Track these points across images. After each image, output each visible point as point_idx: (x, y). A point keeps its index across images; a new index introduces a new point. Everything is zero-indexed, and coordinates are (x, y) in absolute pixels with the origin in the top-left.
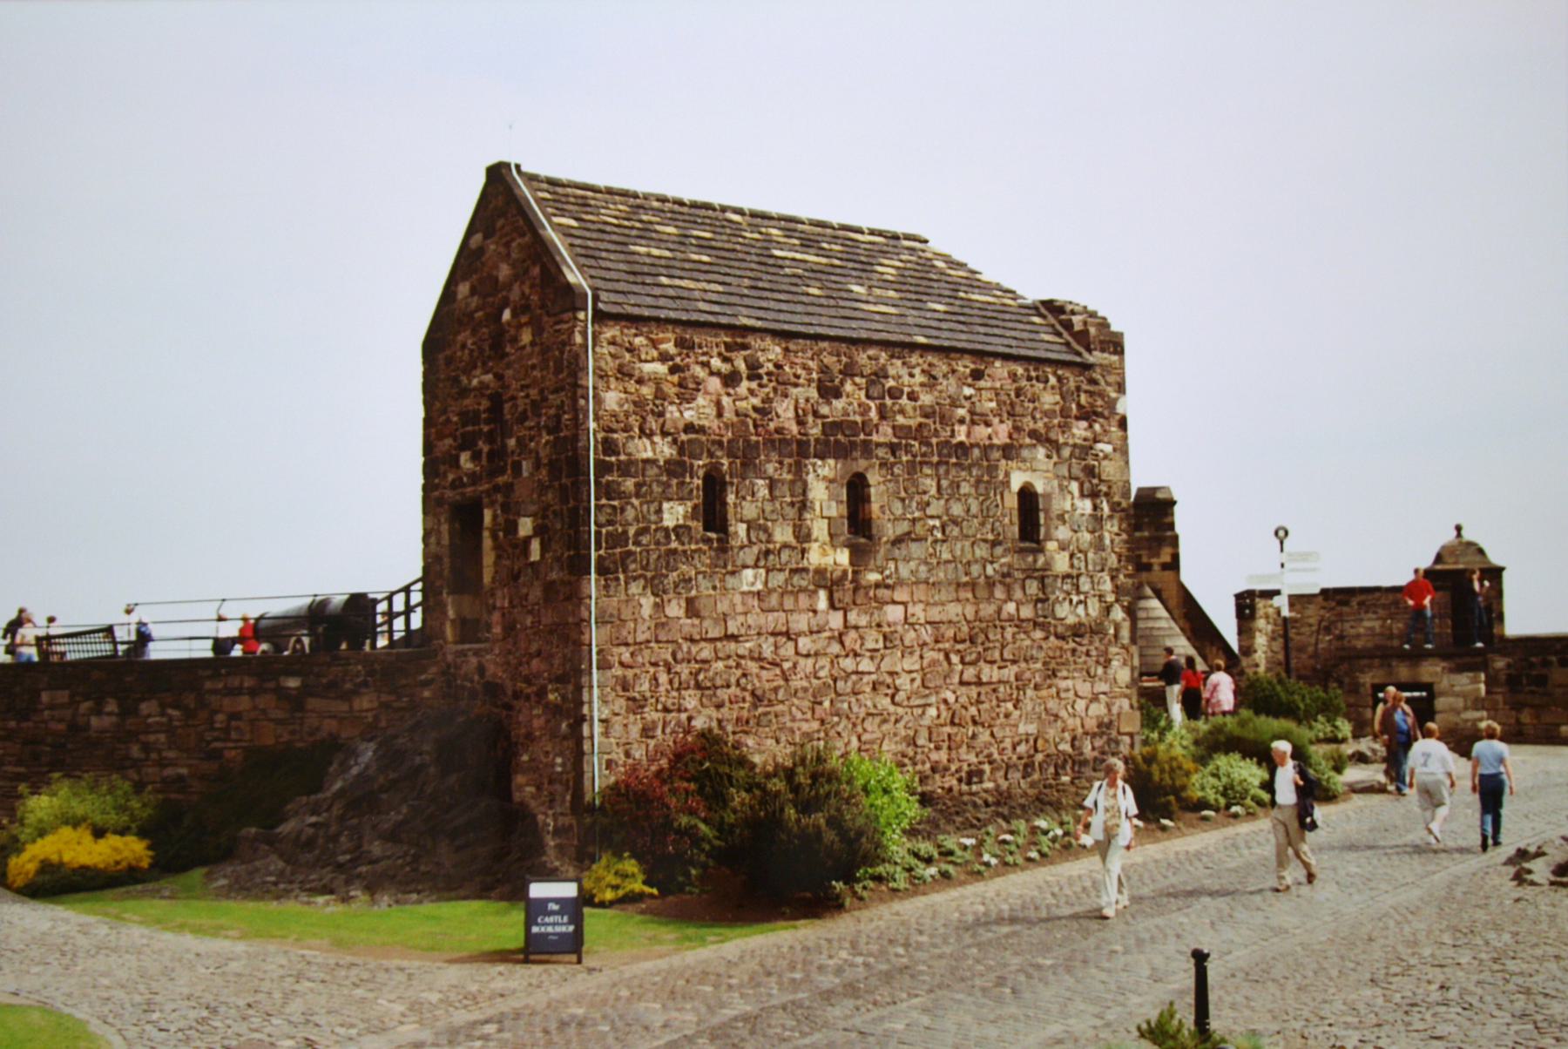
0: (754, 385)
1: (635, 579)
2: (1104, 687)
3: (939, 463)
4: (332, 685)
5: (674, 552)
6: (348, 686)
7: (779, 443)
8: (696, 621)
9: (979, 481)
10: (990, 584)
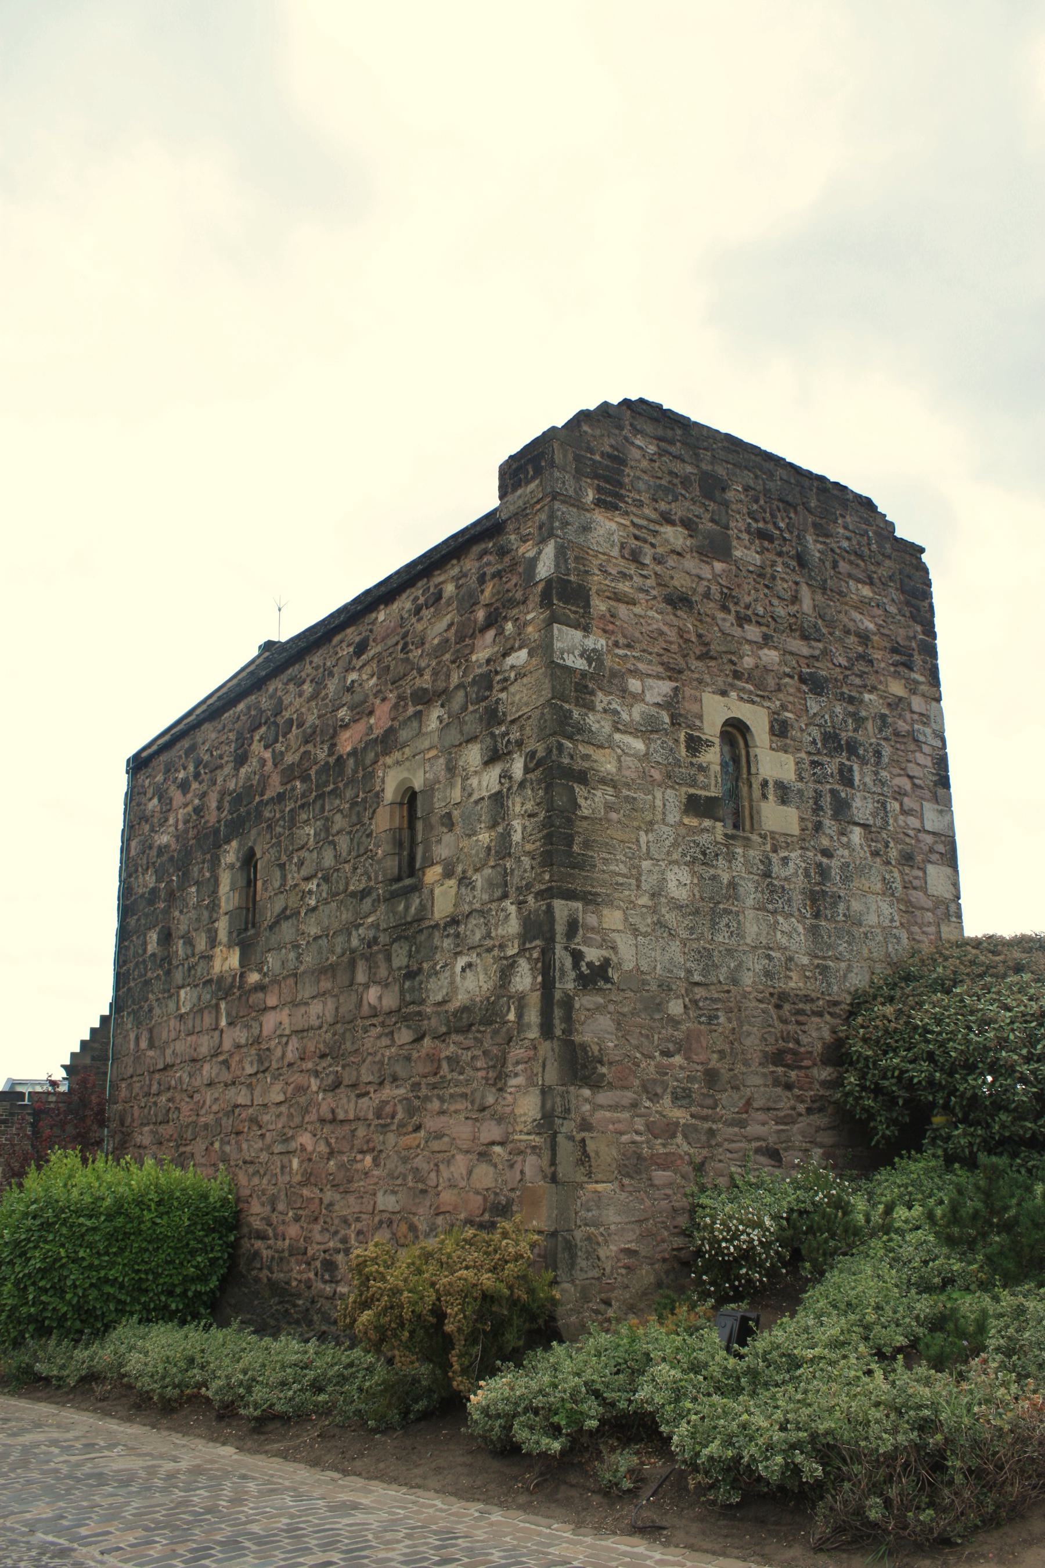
9: (354, 804)
10: (352, 964)
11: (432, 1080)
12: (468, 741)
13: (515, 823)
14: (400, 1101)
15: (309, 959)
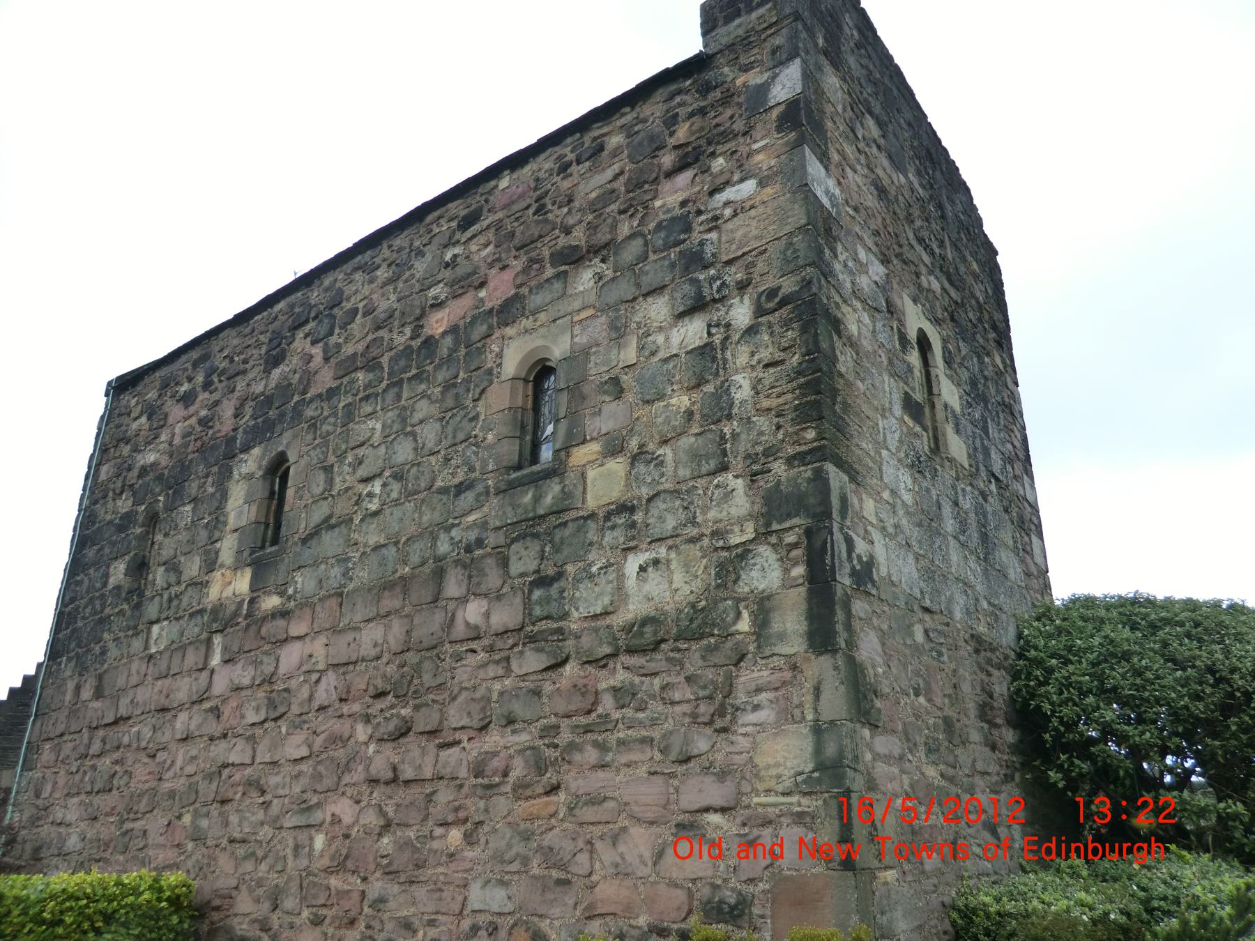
2: (715, 793)
10: (439, 574)
11: (583, 720)
12: (646, 295)
13: (738, 378)
14: (521, 752)
15: (363, 575)
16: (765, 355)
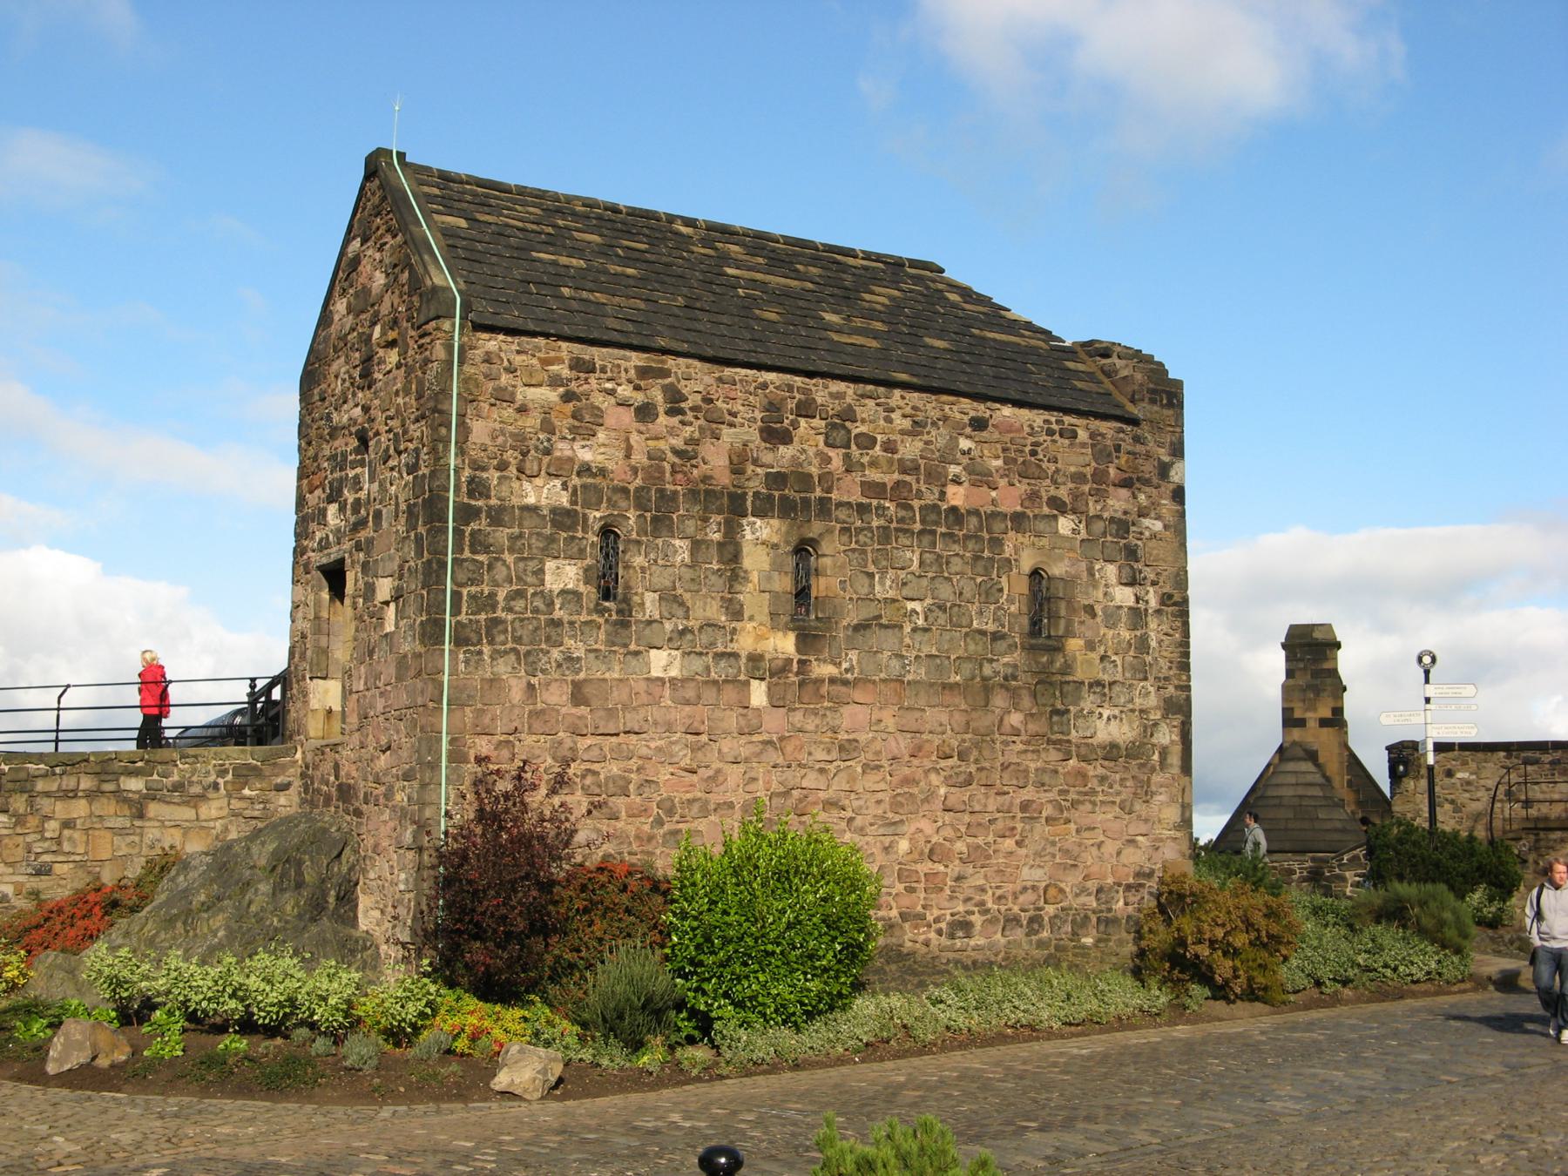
0: (675, 421)
1: (506, 652)
2: (1143, 828)
3: (921, 532)
4: (178, 787)
5: (557, 624)
6: (196, 790)
7: (705, 496)
8: (583, 710)
9: (977, 558)
10: (987, 687)
16: (1165, 628)
